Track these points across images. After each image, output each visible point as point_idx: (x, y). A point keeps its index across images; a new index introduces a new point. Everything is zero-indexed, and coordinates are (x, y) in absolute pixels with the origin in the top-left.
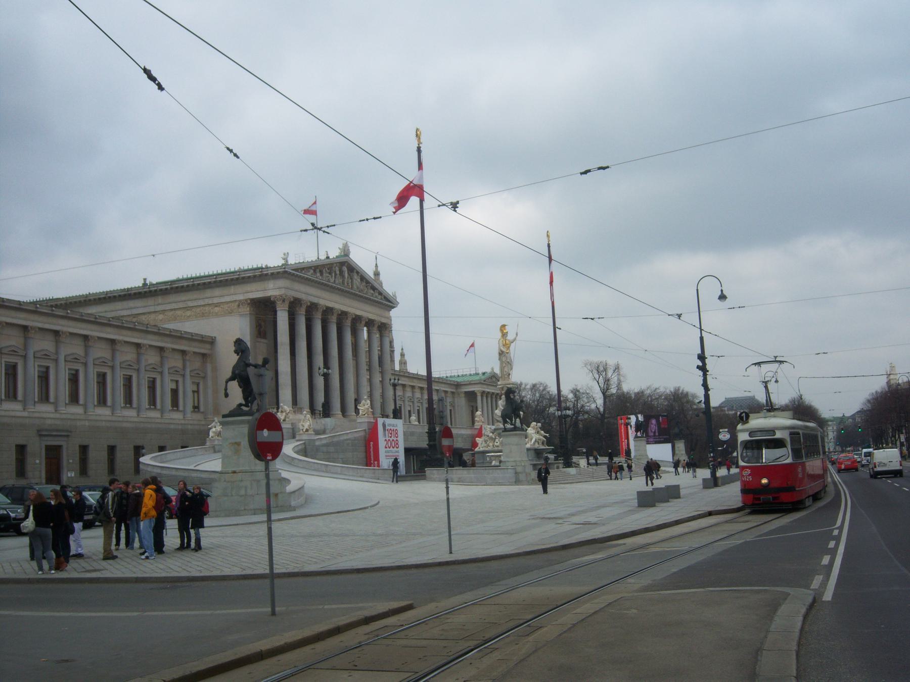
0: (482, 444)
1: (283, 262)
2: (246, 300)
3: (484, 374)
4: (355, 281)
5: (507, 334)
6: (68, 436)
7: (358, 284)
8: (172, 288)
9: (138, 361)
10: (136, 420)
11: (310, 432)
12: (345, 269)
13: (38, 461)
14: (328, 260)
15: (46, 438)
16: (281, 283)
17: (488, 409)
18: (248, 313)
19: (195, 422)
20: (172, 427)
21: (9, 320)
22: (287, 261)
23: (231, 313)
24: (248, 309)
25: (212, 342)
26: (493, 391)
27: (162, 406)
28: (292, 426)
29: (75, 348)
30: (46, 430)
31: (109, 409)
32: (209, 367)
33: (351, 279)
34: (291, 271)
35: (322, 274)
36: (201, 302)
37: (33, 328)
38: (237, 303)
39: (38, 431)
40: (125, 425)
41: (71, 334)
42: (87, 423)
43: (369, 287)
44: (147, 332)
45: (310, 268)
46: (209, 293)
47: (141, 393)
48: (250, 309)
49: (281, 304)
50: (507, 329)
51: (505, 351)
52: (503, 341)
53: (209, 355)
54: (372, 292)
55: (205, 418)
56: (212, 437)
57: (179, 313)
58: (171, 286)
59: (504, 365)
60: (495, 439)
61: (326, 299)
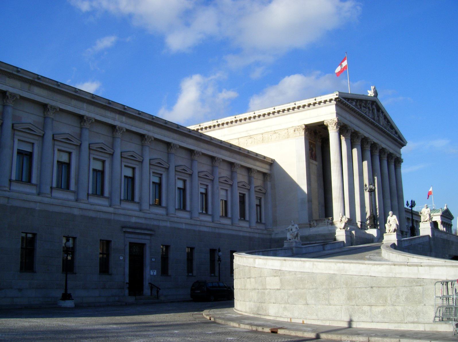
4: (381, 119)
6: (151, 235)
9: (213, 173)
10: (212, 225)
13: (121, 258)
15: (130, 236)
19: (259, 231)
20: (241, 234)
21: (98, 118)
27: (232, 215)
32: (269, 184)
34: (342, 99)
35: (361, 108)
41: (156, 139)
42: (168, 224)
43: (389, 126)
53: (269, 174)
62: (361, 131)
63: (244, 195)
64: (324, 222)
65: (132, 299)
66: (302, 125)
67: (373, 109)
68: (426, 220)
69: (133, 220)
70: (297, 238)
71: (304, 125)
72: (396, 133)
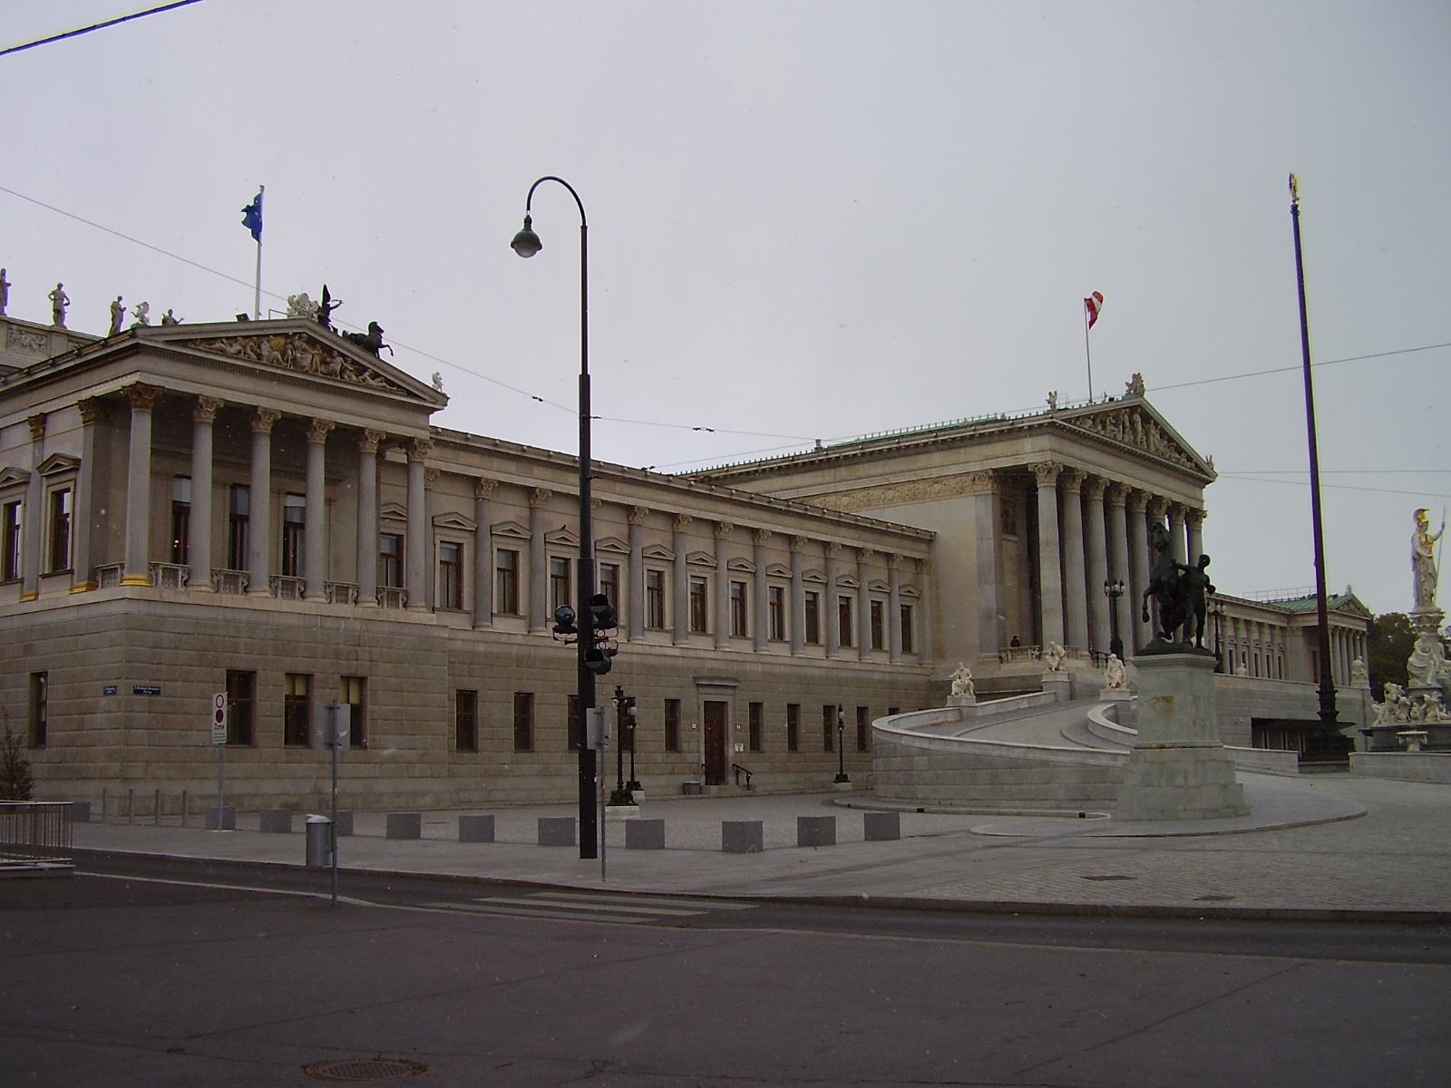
0: (1383, 715)
2: (986, 471)
3: (1335, 596)
4: (1152, 438)
5: (1427, 525)
7: (1157, 443)
10: (825, 664)
11: (1121, 689)
12: (1137, 418)
13: (694, 726)
14: (1112, 404)
16: (1044, 441)
18: (990, 492)
20: (876, 676)
24: (990, 485)
25: (929, 539)
26: (1351, 627)
27: (860, 643)
28: (1069, 678)
29: (738, 550)
30: (705, 678)
31: (787, 646)
32: (925, 579)
33: (1147, 435)
34: (1061, 422)
35: (1104, 427)
37: (685, 517)
38: (971, 477)
39: (695, 678)
40: (811, 672)
42: (760, 668)
44: (839, 524)
45: (1087, 417)
46: (923, 460)
47: (829, 622)
48: (993, 487)
50: (1428, 516)
52: (1420, 538)
56: (956, 694)
60: (1412, 705)
62: (1105, 474)
63: (880, 603)
65: (714, 789)
67: (1132, 423)
69: (709, 664)
70: (968, 692)
72: (1190, 459)
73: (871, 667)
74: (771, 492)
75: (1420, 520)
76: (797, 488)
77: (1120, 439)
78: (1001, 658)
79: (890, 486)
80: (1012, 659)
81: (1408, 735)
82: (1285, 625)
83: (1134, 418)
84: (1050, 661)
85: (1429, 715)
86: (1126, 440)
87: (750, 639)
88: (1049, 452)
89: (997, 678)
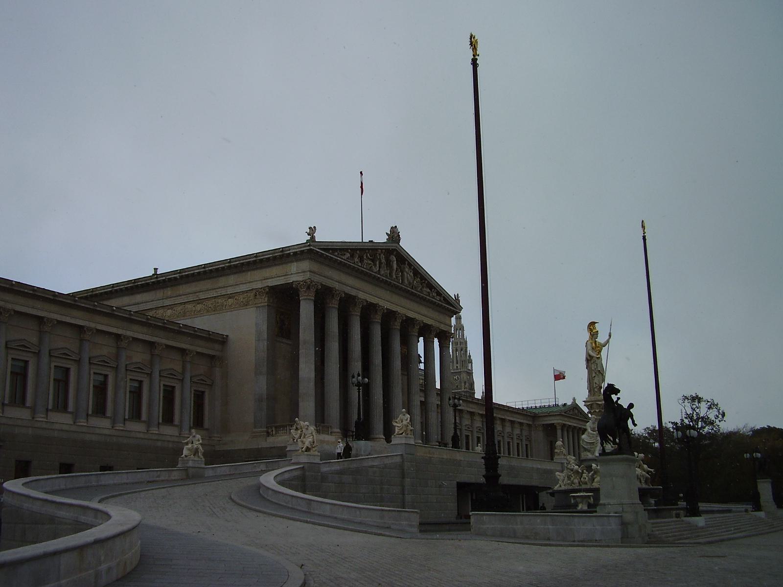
1: (309, 238)
3: (565, 404)
4: (405, 273)
8: (181, 277)
11: (312, 452)
14: (371, 244)
16: (305, 265)
17: (568, 441)
18: (266, 304)
20: (159, 444)
22: (313, 238)
23: (246, 305)
24: (266, 299)
25: (223, 341)
26: (575, 425)
33: (402, 272)
34: (318, 250)
35: (361, 260)
36: (214, 294)
43: (425, 285)
46: (222, 281)
48: (268, 300)
49: (305, 292)
51: (595, 355)
52: (592, 343)
54: (429, 290)
55: (210, 437)
57: (189, 306)
58: (180, 275)
59: (594, 375)
60: (583, 473)
61: (367, 293)
64: (286, 429)
66: (265, 287)
68: (401, 432)
71: (267, 288)
73: (155, 437)
74: (125, 306)
75: (592, 331)
76: (138, 304)
77: (375, 271)
78: (268, 432)
79: (199, 301)
80: (276, 433)
81: (578, 496)
82: (531, 423)
83: (391, 258)
84: (294, 434)
85: (596, 480)
86: (382, 272)
87: (28, 408)
88: (309, 273)
89: (261, 448)
